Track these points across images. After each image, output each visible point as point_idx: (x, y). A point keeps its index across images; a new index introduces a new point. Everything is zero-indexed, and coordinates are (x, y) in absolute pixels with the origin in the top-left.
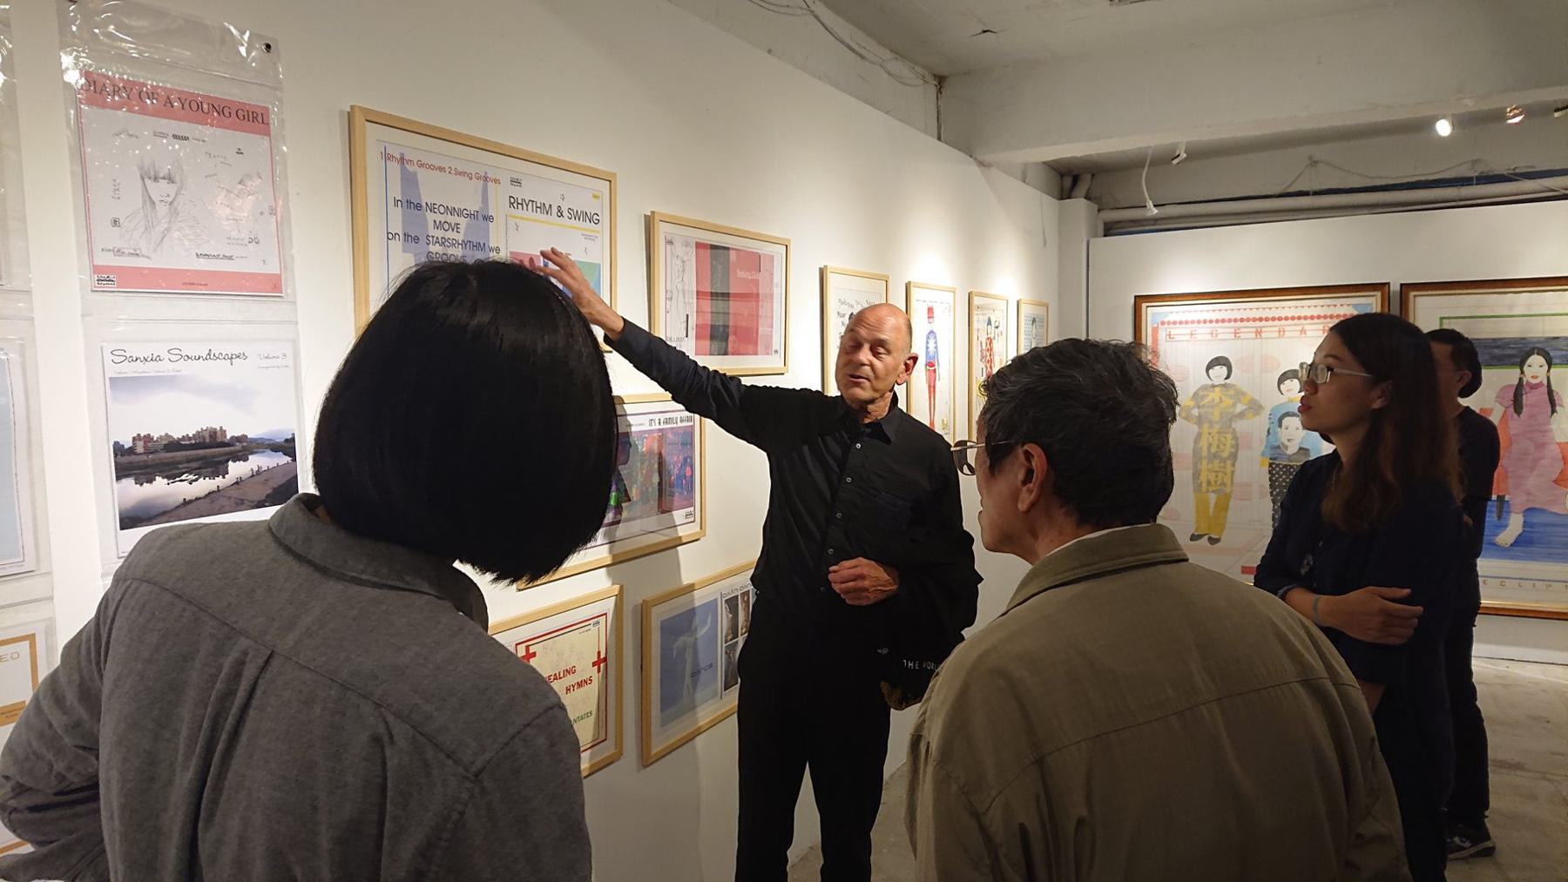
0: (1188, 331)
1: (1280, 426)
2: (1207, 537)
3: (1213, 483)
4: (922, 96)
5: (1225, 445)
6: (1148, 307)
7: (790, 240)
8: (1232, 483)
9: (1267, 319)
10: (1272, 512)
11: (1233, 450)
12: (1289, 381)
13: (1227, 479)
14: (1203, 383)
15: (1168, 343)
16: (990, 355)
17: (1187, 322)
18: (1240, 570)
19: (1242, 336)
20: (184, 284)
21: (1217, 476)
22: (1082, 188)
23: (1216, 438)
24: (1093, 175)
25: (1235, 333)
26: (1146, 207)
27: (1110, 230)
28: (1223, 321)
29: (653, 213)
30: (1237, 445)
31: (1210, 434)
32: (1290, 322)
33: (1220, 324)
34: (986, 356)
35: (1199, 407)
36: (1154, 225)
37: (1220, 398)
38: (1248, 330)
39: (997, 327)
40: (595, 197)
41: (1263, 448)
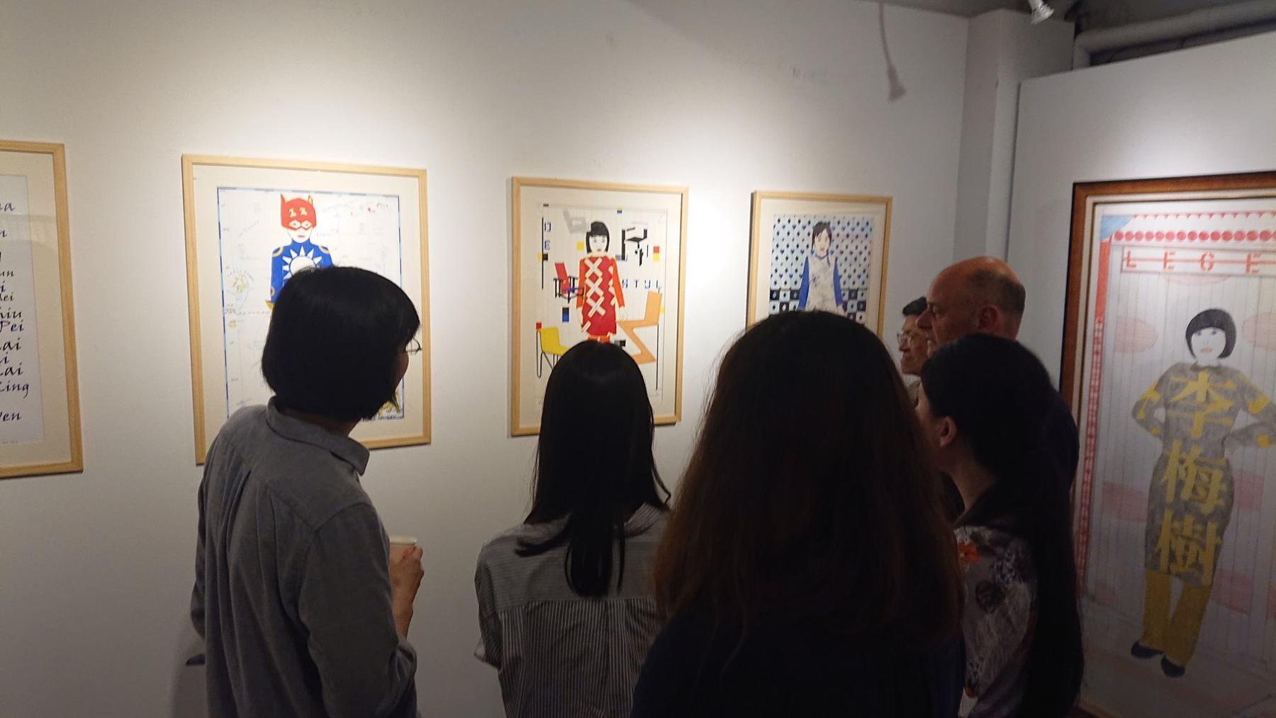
0: (1160, 254)
3: (1179, 559)
5: (1207, 490)
6: (1095, 204)
8: (1214, 569)
11: (1221, 502)
13: (1206, 560)
14: (1178, 360)
15: (1125, 275)
16: (604, 286)
17: (1159, 236)
21: (1187, 548)
23: (1192, 475)
25: (1249, 263)
27: (1099, 57)
30: (1231, 495)
31: (1182, 462)
33: (1220, 243)
34: (583, 290)
35: (1167, 406)
37: (1207, 392)
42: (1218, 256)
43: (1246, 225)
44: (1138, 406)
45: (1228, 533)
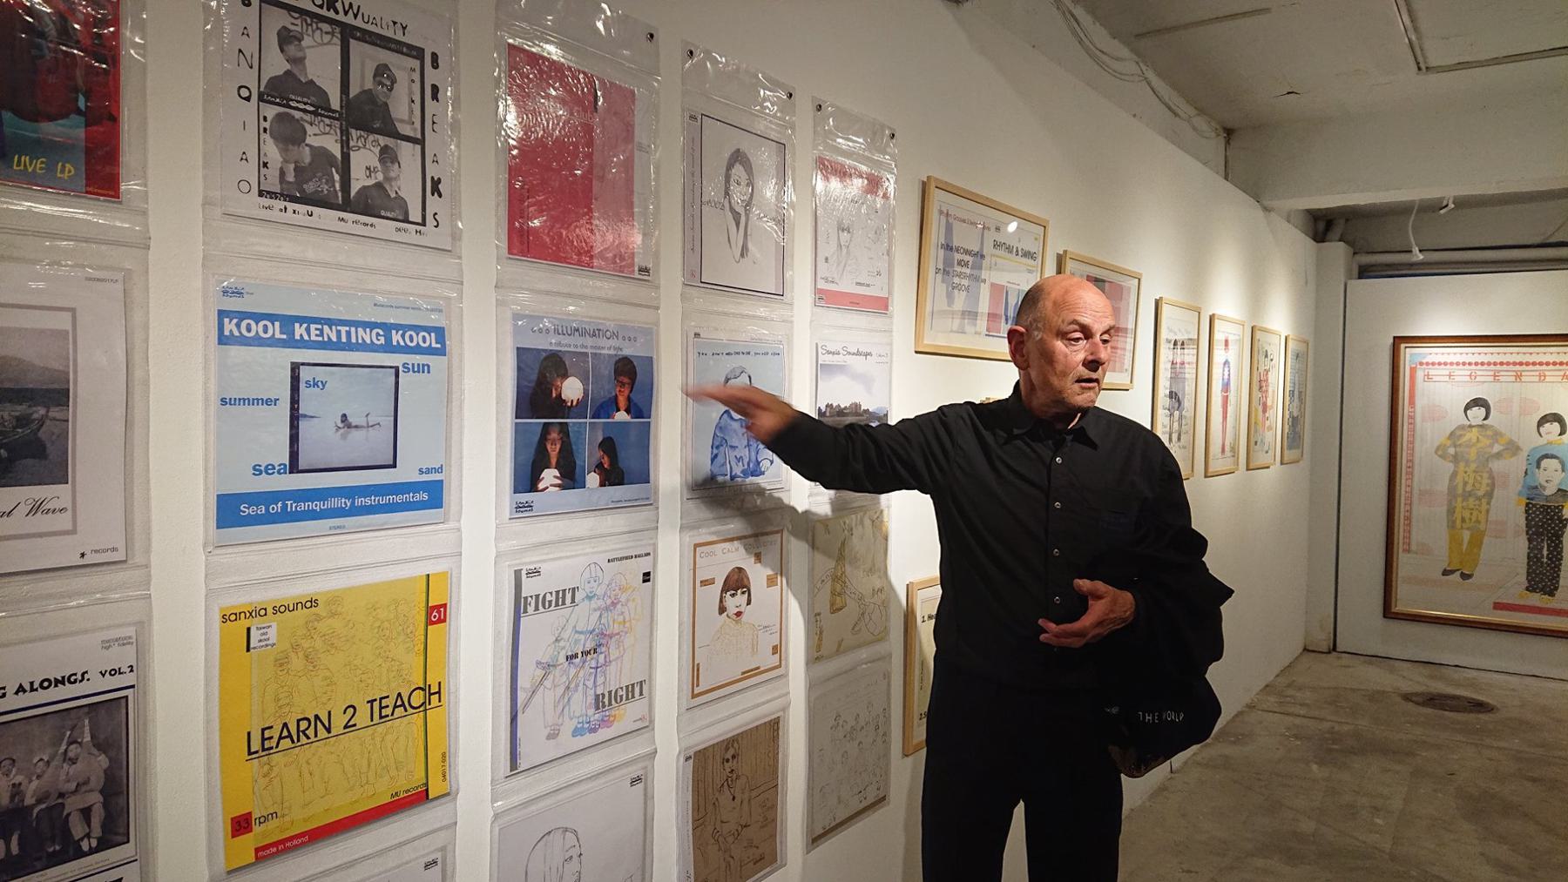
1: (1538, 466)
2: (1458, 573)
4: (1215, 145)
5: (1480, 483)
6: (1406, 347)
7: (1141, 274)
8: (1487, 521)
9: (1527, 364)
10: (1527, 551)
11: (1488, 488)
12: (1549, 424)
13: (1482, 517)
17: (1445, 364)
18: (1492, 606)
19: (1502, 379)
20: (851, 303)
21: (1471, 514)
22: (1338, 230)
24: (1347, 220)
25: (1495, 376)
26: (1411, 251)
27: (1365, 272)
28: (1482, 364)
29: (1065, 252)
30: (1493, 484)
32: (1551, 367)
33: (1479, 367)
35: (1455, 446)
36: (1410, 269)
38: (1507, 376)
39: (1272, 360)
40: (1036, 239)
41: (1520, 488)
42: (1479, 373)
43: (1492, 359)
44: (1438, 449)
45: (1493, 501)
